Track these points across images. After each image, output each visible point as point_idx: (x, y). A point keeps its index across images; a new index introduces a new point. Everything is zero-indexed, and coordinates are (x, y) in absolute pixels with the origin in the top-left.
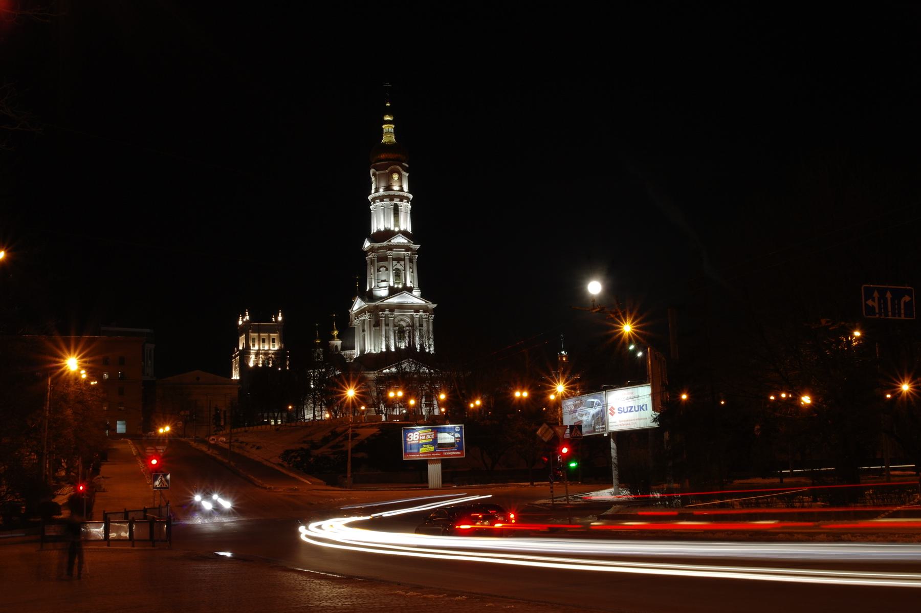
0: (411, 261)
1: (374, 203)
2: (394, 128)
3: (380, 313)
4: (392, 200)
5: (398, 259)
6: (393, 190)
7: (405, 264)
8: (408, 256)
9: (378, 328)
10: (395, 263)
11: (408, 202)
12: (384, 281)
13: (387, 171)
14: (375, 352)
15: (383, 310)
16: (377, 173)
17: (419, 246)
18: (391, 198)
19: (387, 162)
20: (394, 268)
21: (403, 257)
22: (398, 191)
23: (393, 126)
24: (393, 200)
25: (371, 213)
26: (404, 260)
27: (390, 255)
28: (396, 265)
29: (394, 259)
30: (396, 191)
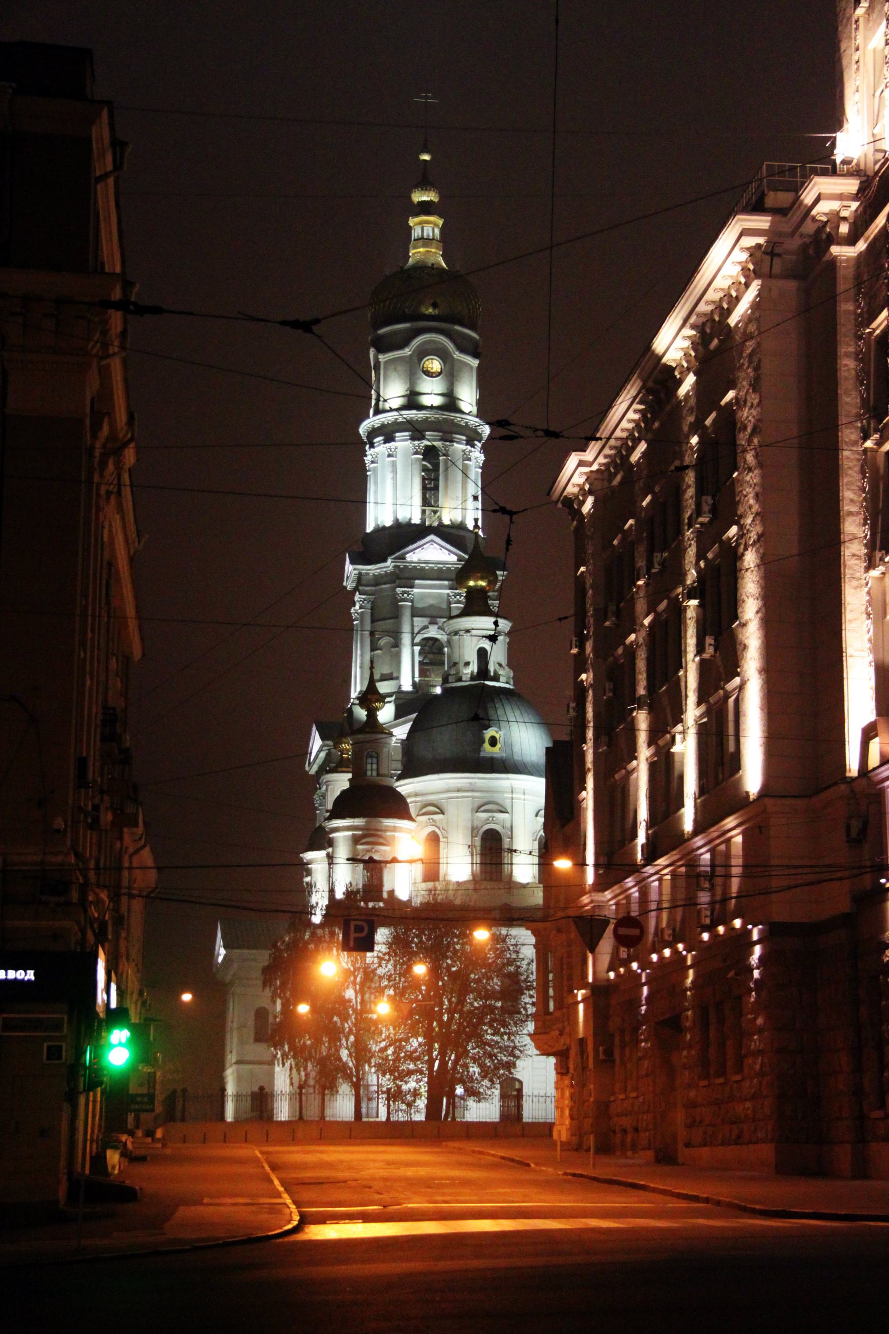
1: (372, 446)
2: (443, 230)
5: (433, 614)
6: (420, 407)
8: (458, 602)
10: (419, 622)
11: (470, 442)
13: (407, 351)
16: (382, 358)
20: (418, 639)
22: (440, 408)
23: (441, 222)
24: (423, 438)
25: (367, 476)
28: (425, 627)
29: (416, 612)
30: (432, 407)
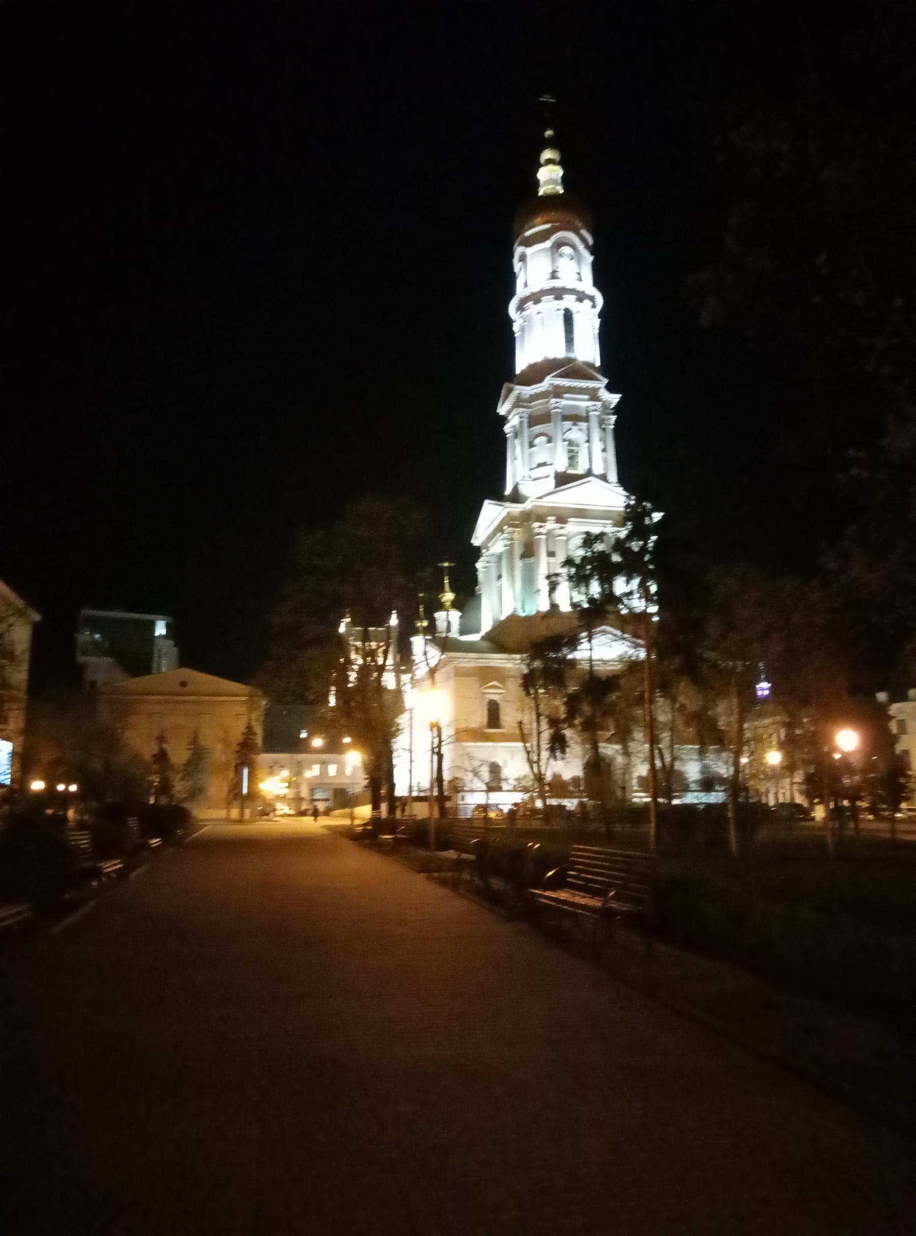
0: (601, 422)
3: (536, 524)
4: (559, 297)
5: (575, 418)
7: (588, 429)
9: (531, 560)
10: (567, 424)
12: (544, 464)
14: (523, 615)
15: (542, 519)
17: (619, 396)
18: (558, 293)
19: (548, 226)
21: (584, 414)
26: (586, 419)
27: (557, 408)
28: (570, 429)
29: (565, 418)
